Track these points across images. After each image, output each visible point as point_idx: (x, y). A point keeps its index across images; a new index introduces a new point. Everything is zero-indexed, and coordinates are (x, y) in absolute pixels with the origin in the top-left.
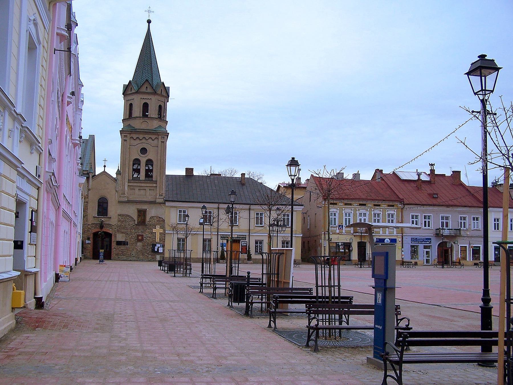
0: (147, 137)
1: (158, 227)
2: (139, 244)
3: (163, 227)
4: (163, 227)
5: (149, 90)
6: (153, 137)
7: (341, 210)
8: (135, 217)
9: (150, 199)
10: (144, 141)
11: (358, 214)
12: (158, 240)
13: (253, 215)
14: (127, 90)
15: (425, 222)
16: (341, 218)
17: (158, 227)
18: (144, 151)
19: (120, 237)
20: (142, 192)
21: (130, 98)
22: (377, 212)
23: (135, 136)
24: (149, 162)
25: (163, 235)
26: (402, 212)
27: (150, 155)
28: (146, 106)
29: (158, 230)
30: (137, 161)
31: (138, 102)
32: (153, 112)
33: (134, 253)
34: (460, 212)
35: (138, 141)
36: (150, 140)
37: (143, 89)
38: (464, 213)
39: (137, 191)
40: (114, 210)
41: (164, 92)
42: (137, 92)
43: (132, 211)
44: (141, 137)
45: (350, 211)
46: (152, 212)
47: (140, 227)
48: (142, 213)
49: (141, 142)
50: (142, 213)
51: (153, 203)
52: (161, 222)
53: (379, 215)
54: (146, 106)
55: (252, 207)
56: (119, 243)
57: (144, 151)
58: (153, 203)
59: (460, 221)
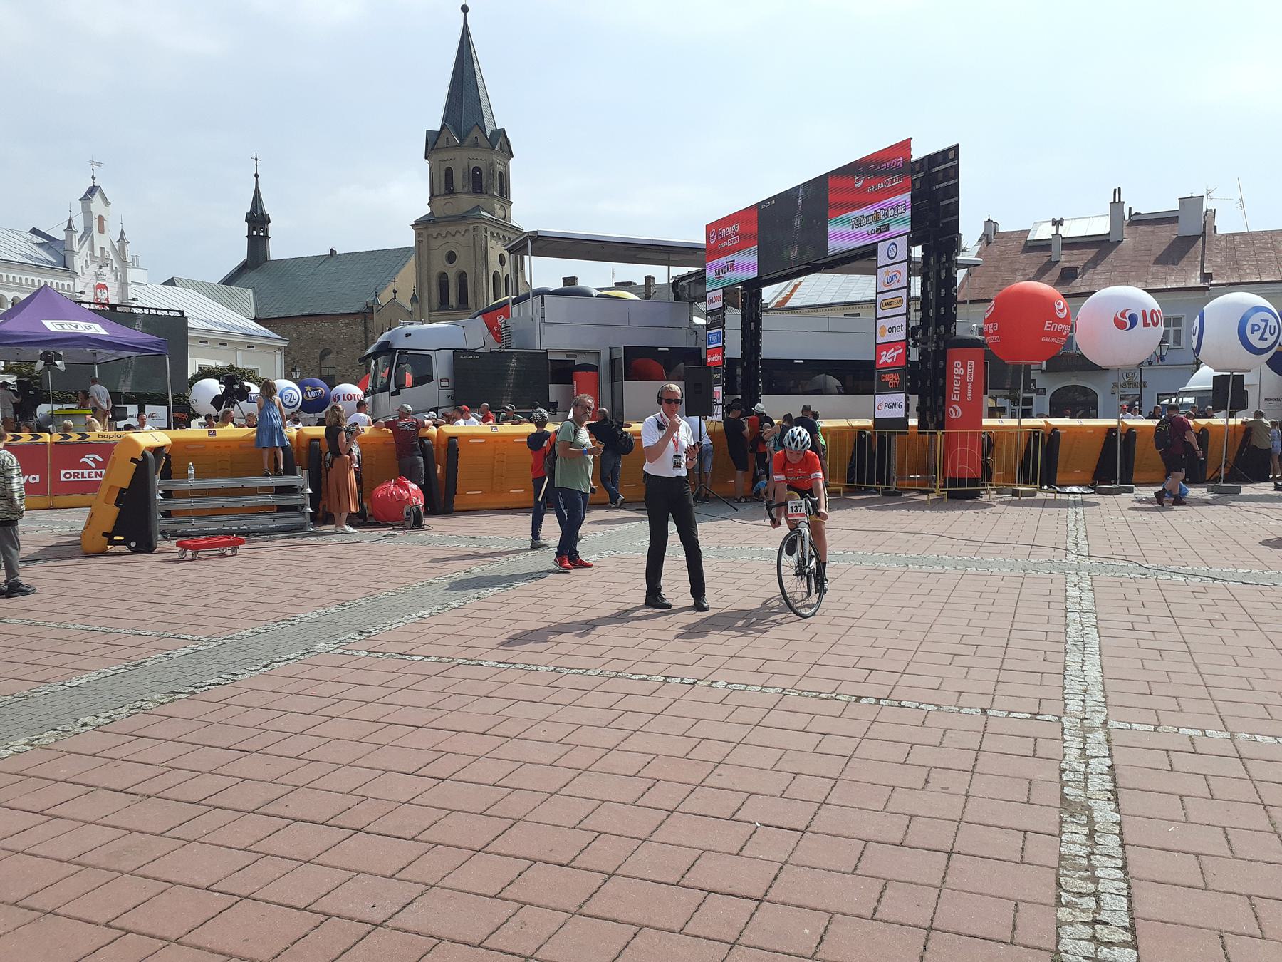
0: (452, 229)
6: (462, 228)
10: (450, 238)
14: (434, 144)
18: (451, 257)
21: (440, 156)
23: (434, 231)
27: (461, 264)
36: (458, 235)
44: (444, 231)
49: (446, 240)
57: (451, 257)
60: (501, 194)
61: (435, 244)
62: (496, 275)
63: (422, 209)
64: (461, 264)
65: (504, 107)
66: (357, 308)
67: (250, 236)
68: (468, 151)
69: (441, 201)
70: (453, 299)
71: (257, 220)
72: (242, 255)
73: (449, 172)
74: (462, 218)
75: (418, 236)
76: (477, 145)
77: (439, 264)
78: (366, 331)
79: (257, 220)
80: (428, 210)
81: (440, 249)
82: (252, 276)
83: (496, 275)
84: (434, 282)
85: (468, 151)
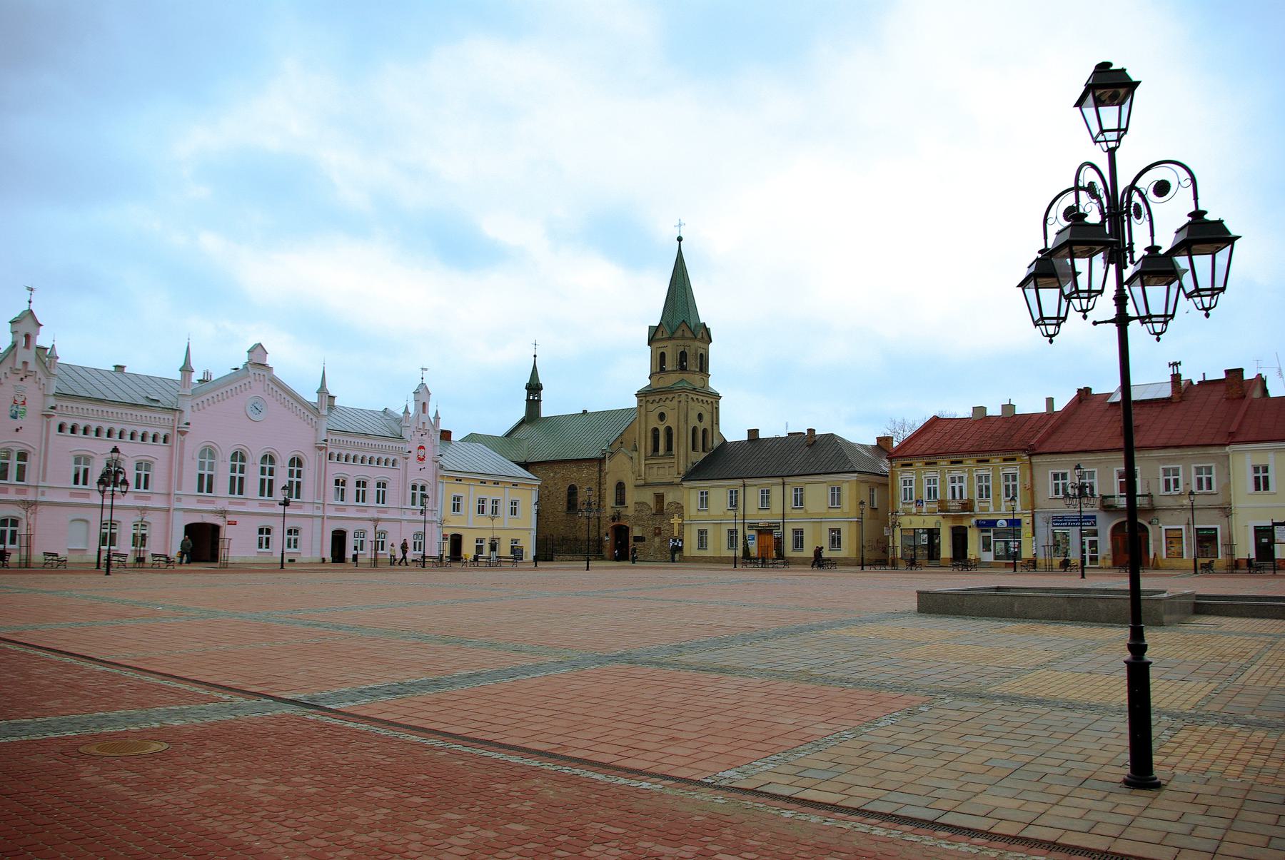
0: (664, 397)
1: (676, 516)
2: (657, 539)
3: (681, 516)
4: (681, 516)
5: (690, 335)
6: (670, 396)
7: (943, 474)
8: (652, 503)
9: (668, 479)
11: (949, 479)
12: (676, 534)
13: (790, 492)
14: (655, 336)
15: (953, 488)
16: (919, 487)
17: (676, 516)
19: (636, 532)
20: (661, 471)
22: (956, 474)
23: (651, 399)
24: (669, 431)
25: (681, 525)
26: (1031, 469)
27: (670, 421)
28: (683, 356)
29: (676, 520)
30: (655, 430)
31: (671, 350)
32: (692, 364)
33: (651, 551)
34: (1160, 460)
35: (655, 405)
37: (679, 333)
38: (1170, 460)
39: (655, 470)
40: (631, 497)
41: (705, 335)
42: (670, 338)
43: (648, 496)
44: (657, 398)
45: (933, 474)
46: (670, 497)
47: (658, 517)
48: (660, 498)
50: (660, 498)
51: (671, 484)
52: (679, 509)
53: (987, 477)
54: (683, 356)
55: (787, 480)
56: (637, 539)
58: (671, 484)
59: (990, 484)
60: (701, 370)
61: (651, 407)
62: (694, 430)
63: (643, 380)
64: (670, 421)
65: (707, 309)
66: (596, 454)
67: (528, 400)
68: (680, 339)
69: (656, 378)
70: (662, 450)
71: (534, 388)
72: (521, 413)
73: (663, 355)
74: (670, 390)
75: (640, 401)
76: (683, 337)
77: (654, 422)
78: (600, 471)
79: (534, 388)
80: (649, 382)
81: (655, 410)
82: (526, 431)
83: (694, 430)
84: (649, 434)
85: (680, 339)
